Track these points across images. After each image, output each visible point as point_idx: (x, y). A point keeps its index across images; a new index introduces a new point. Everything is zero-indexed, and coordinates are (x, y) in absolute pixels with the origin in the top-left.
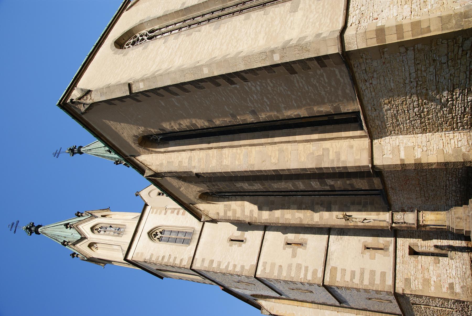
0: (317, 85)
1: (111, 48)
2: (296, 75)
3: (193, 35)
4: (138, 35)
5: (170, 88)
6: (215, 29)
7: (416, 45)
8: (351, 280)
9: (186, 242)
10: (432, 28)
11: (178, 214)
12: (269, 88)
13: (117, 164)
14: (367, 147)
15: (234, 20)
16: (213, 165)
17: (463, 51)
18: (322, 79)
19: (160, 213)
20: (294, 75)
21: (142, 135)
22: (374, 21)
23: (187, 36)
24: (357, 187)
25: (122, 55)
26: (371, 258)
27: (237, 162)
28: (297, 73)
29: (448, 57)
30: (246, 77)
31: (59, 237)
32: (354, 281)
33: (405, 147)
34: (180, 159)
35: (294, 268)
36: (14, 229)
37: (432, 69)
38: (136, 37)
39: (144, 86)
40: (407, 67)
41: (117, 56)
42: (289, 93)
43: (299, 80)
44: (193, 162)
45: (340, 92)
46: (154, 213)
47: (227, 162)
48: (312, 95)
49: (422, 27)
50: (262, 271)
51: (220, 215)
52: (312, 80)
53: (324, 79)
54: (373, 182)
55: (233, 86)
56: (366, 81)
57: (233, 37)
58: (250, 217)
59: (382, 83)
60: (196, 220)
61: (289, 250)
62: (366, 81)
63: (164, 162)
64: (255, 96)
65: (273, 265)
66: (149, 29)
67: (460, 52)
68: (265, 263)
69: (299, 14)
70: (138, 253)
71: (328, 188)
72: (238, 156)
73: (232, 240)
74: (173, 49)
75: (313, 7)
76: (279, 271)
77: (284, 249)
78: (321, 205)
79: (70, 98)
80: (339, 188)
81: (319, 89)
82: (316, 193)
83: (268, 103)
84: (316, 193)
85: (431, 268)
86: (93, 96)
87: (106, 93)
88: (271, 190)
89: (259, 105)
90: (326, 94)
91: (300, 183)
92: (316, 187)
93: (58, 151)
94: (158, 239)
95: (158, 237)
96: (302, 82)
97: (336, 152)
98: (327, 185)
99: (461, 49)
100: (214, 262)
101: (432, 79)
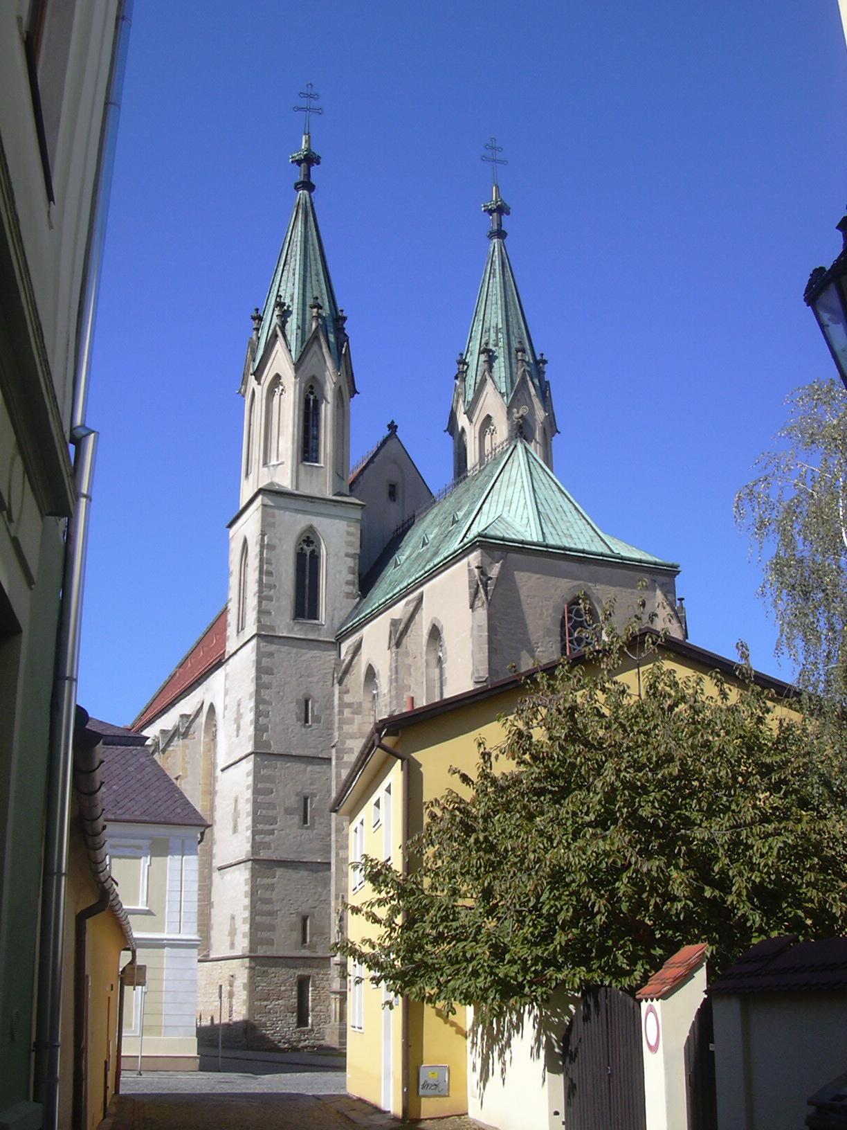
11: (348, 583)
35: (270, 813)
36: (303, 103)
51: (345, 695)
61: (293, 802)
63: (411, 659)
73: (307, 702)
77: (297, 795)
93: (499, 156)
94: (302, 549)
95: (305, 547)
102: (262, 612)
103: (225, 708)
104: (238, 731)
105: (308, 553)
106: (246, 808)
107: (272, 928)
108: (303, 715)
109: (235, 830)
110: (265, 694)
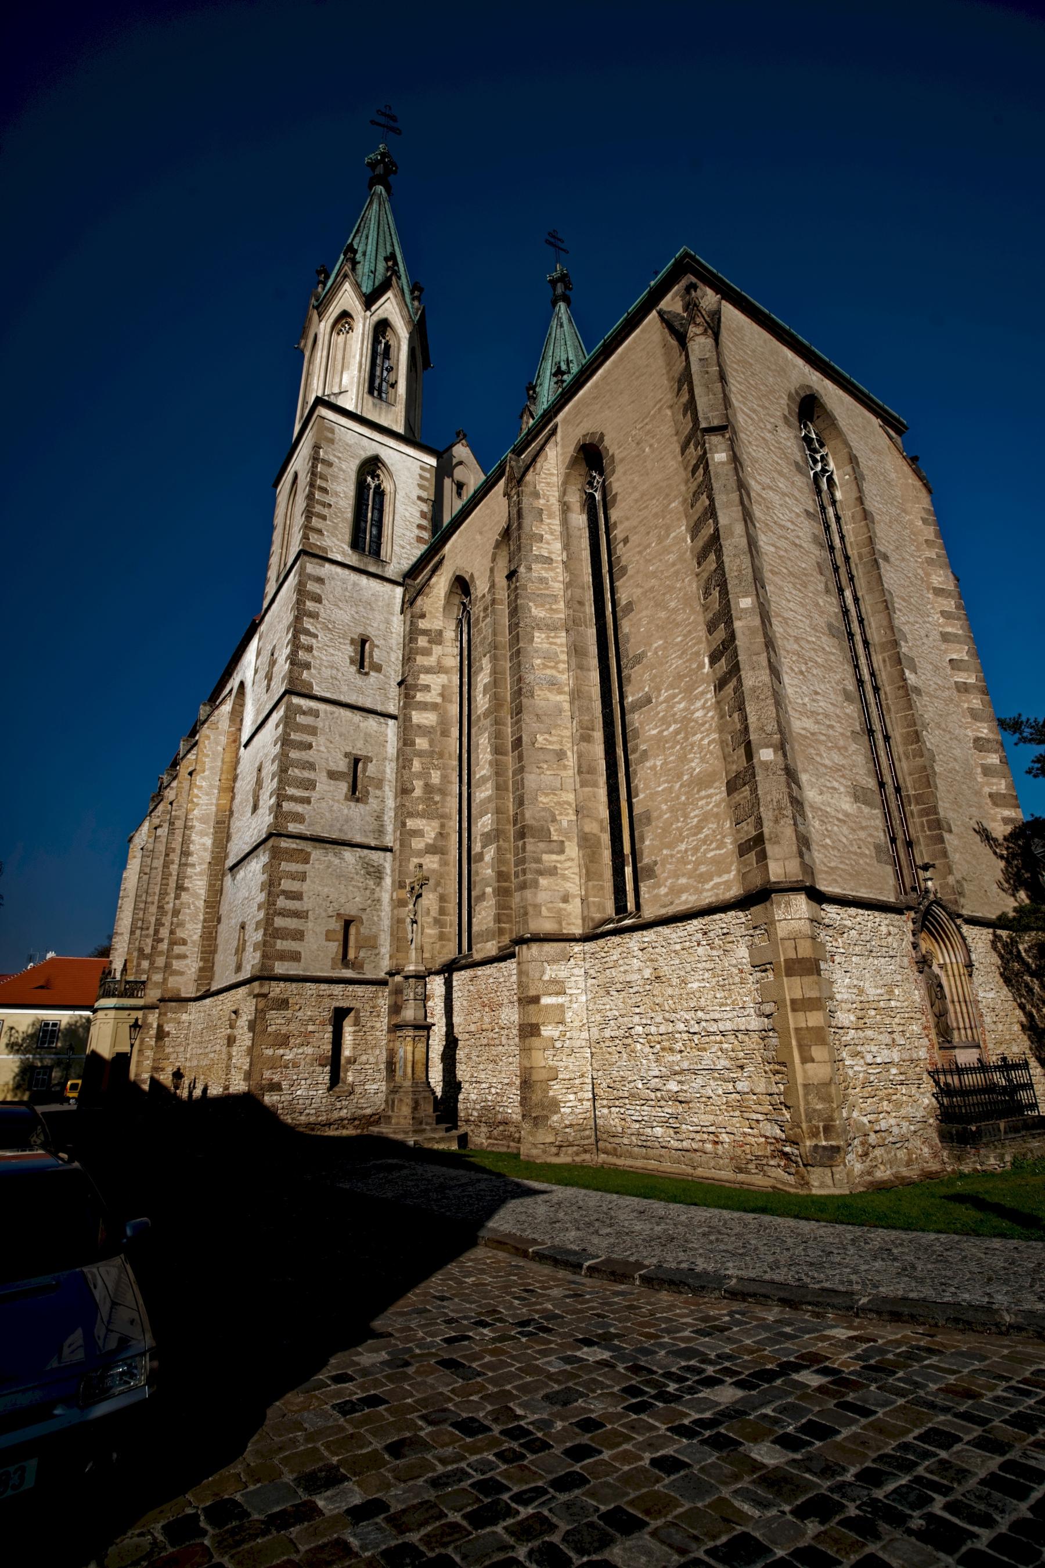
0: (702, 836)
1: (802, 387)
2: (725, 794)
3: (819, 577)
4: (823, 452)
5: (711, 521)
6: (830, 626)
7: (776, 1035)
8: (284, 892)
9: (356, 544)
10: (809, 1065)
11: (420, 527)
12: (699, 736)
13: (528, 389)
14: (565, 931)
15: (846, 667)
16: (533, 610)
17: (758, 1121)
18: (714, 845)
19: (421, 486)
20: (724, 789)
21: (604, 454)
22: (828, 956)
23: (818, 563)
24: (477, 908)
25: (786, 413)
26: (328, 931)
27: (538, 661)
28: (728, 795)
29: (748, 1093)
30: (727, 687)
31: (363, 238)
32: (282, 897)
33: (562, 1005)
34: (547, 537)
35: (306, 774)
37: (724, 1063)
38: (822, 445)
39: (719, 463)
40: (730, 1015)
41: (784, 401)
42: (686, 777)
43: (713, 799)
44: (540, 565)
45: (683, 881)
46: (421, 472)
47: (539, 640)
48: (679, 824)
49: (813, 1048)
50: (300, 707)
52: (710, 826)
53: (713, 850)
54: (487, 941)
55: (706, 660)
56: (705, 933)
57: (810, 664)
58: (416, 685)
59: (699, 965)
60: (406, 565)
62: (705, 933)
63: (542, 501)
64: (682, 706)
65: (313, 731)
66: (835, 477)
67: (755, 1116)
68: (316, 714)
69: (847, 805)
70: (332, 431)
71: (477, 848)
72: (552, 664)
74: (793, 531)
75: (862, 834)
76: (301, 743)
78: (441, 834)
79: (700, 284)
80: (477, 872)
81: (691, 839)
82: (465, 825)
83: (665, 733)
84: (465, 825)
85: (309, 1050)
86: (702, 339)
87: (707, 373)
88: (473, 731)
89: (661, 714)
90: (679, 852)
91: (489, 793)
92: (479, 824)
93: (559, 244)
96: (708, 804)
97: (556, 868)
98: (483, 847)
99: (760, 1117)
100: (317, 605)
101: (703, 1062)
102: (307, 528)
103: (256, 672)
104: (268, 686)
105: (373, 486)
106: (270, 768)
107: (298, 935)
108: (358, 657)
109: (255, 808)
110: (308, 624)
